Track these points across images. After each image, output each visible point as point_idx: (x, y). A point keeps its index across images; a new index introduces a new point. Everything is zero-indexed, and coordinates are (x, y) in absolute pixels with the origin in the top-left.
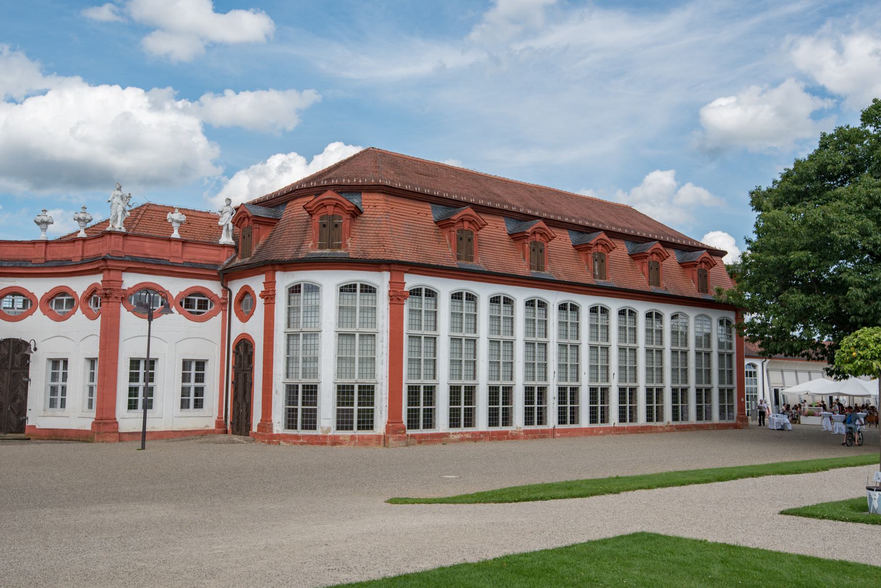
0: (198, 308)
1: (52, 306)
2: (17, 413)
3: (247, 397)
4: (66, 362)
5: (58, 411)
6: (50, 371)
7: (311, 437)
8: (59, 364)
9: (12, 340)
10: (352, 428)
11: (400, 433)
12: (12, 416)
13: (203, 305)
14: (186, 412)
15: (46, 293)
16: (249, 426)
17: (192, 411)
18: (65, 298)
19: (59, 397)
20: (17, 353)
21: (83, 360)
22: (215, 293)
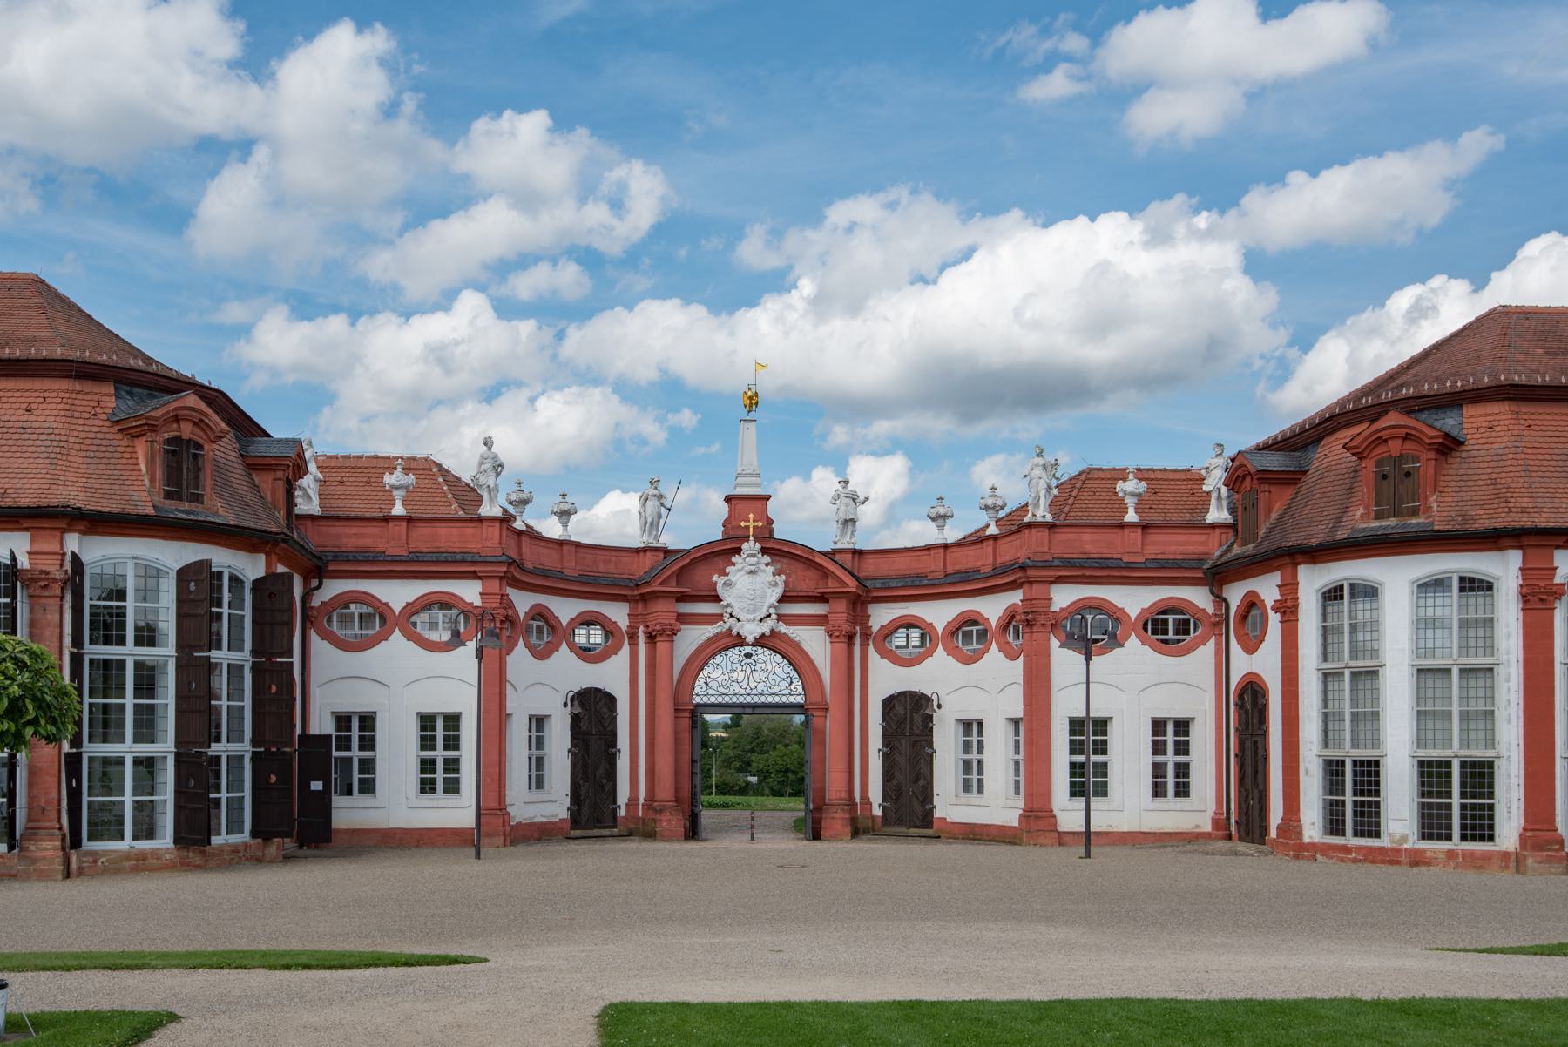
1: (957, 639)
2: (921, 799)
3: (1260, 776)
4: (980, 724)
5: (974, 797)
6: (961, 738)
7: (1370, 849)
8: (973, 727)
9: (908, 694)
10: (1449, 838)
12: (915, 803)
14: (1160, 803)
16: (1265, 829)
17: (1170, 801)
18: (974, 628)
19: (975, 777)
20: (916, 713)
21: (1004, 720)
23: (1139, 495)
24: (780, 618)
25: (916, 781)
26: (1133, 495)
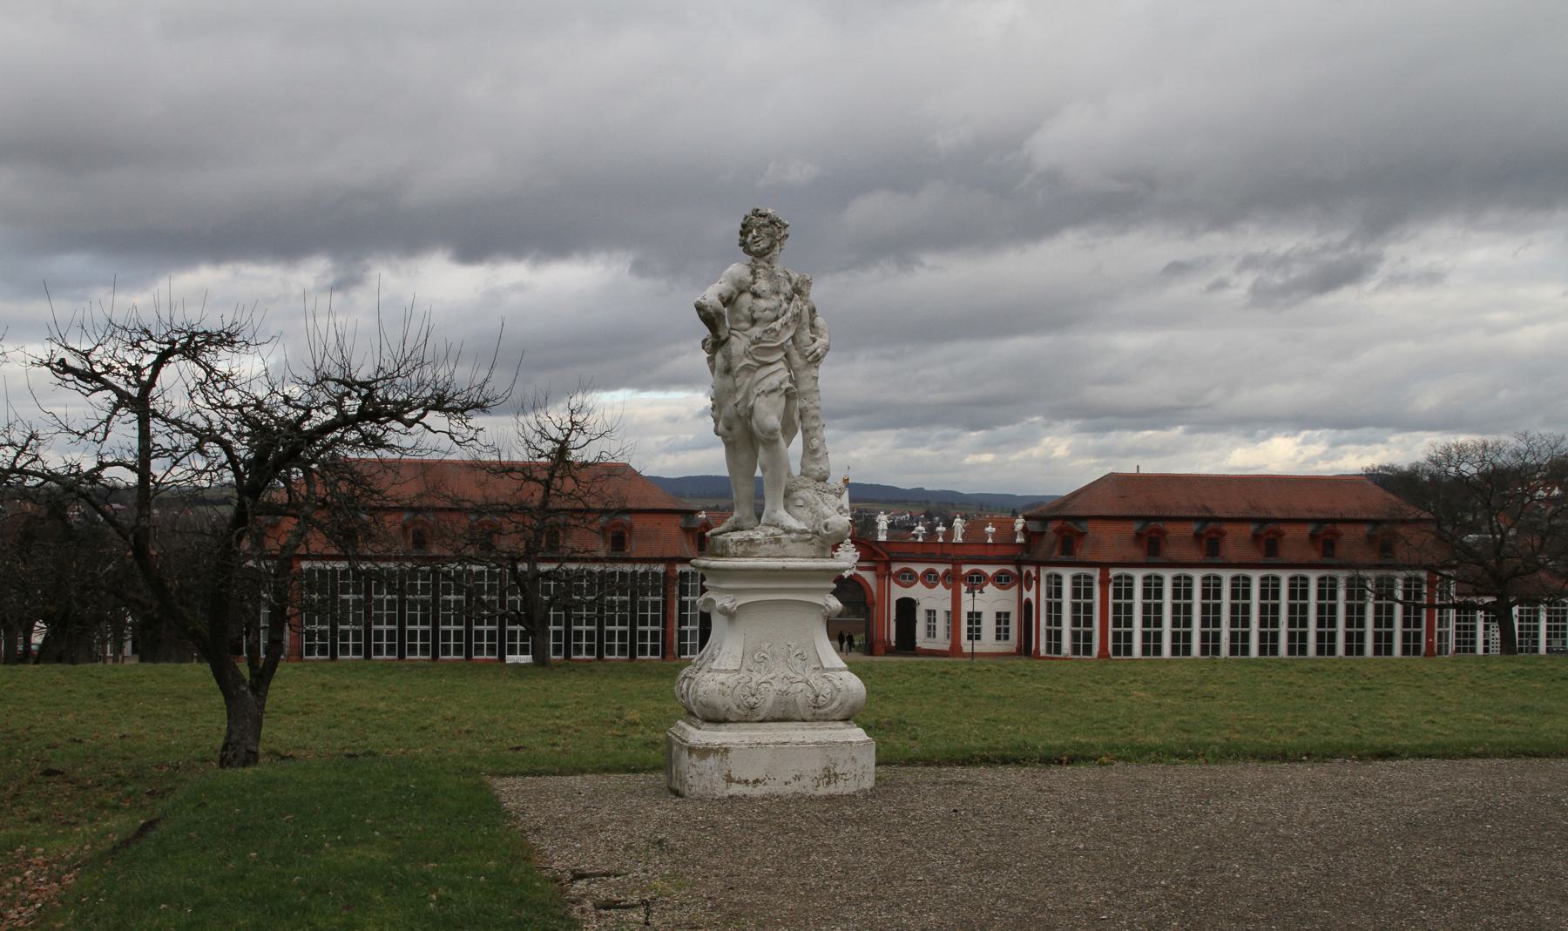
4: (935, 611)
5: (932, 640)
8: (931, 613)
14: (1000, 642)
23: (993, 533)
24: (858, 568)
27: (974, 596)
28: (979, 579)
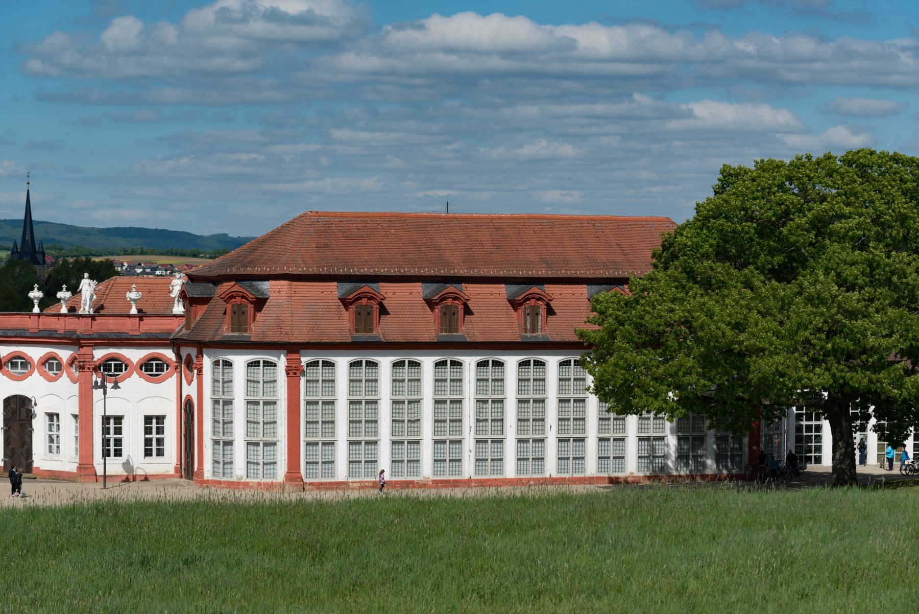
0: (156, 371)
1: (46, 368)
4: (58, 415)
5: (54, 455)
6: (48, 422)
8: (52, 416)
11: (297, 481)
12: (23, 459)
13: (160, 368)
15: (41, 358)
18: (55, 362)
22: (169, 357)
25: (23, 446)
26: (135, 300)
27: (105, 393)
28: (118, 368)
